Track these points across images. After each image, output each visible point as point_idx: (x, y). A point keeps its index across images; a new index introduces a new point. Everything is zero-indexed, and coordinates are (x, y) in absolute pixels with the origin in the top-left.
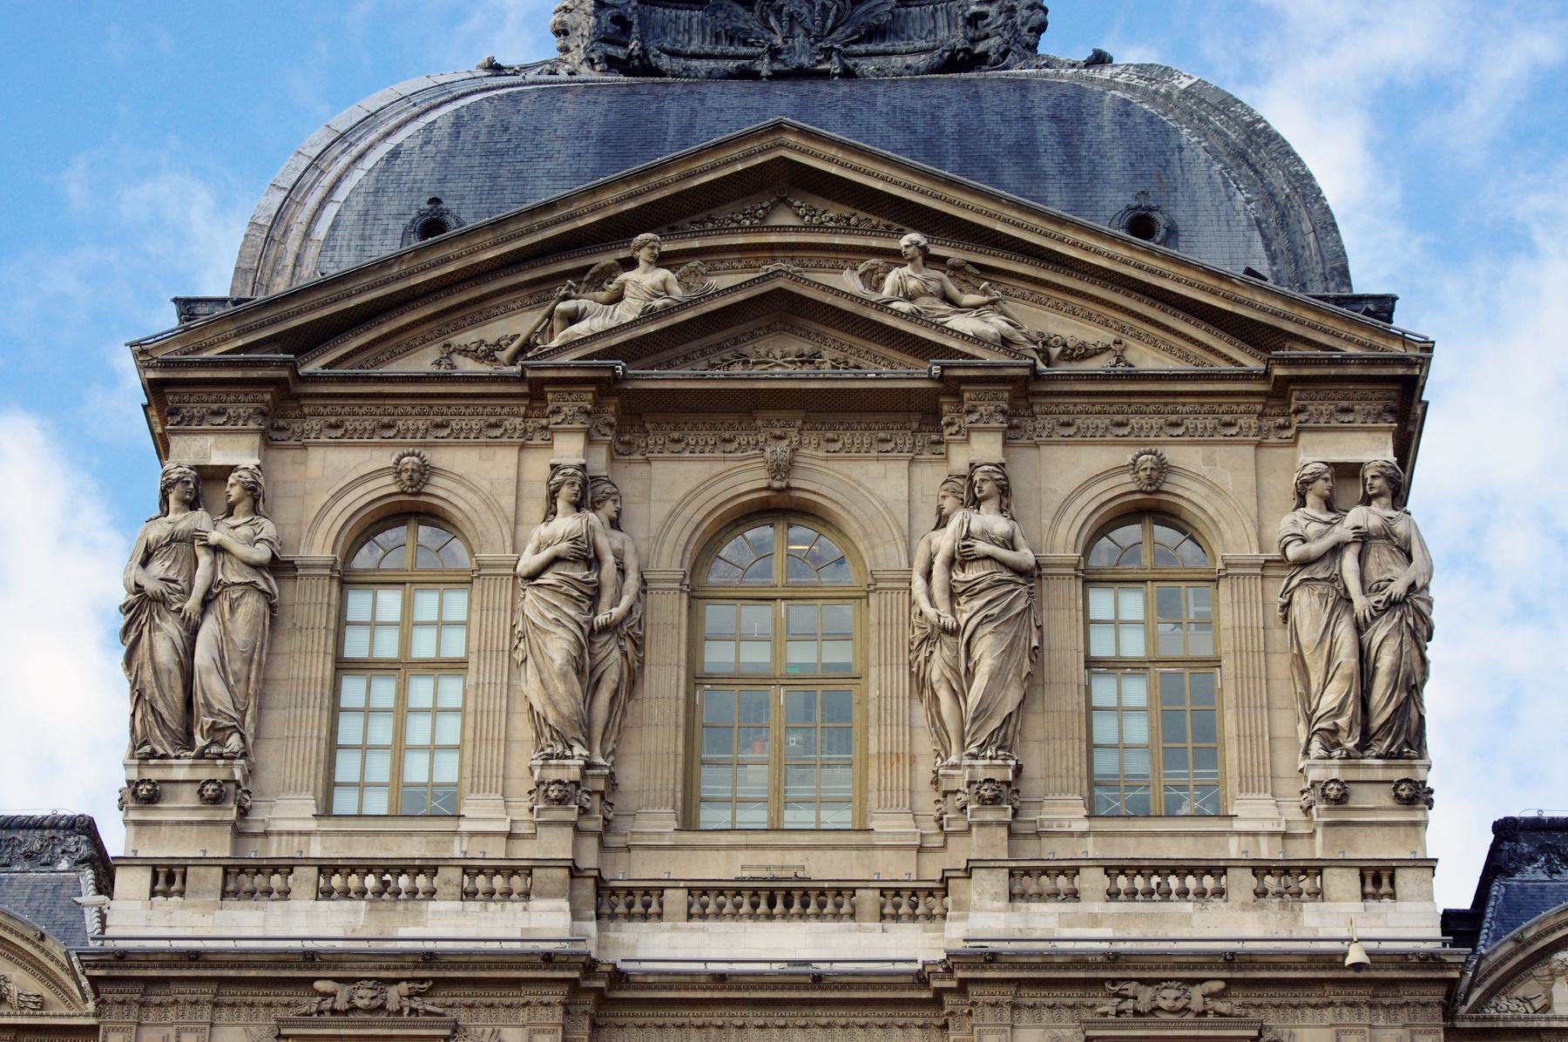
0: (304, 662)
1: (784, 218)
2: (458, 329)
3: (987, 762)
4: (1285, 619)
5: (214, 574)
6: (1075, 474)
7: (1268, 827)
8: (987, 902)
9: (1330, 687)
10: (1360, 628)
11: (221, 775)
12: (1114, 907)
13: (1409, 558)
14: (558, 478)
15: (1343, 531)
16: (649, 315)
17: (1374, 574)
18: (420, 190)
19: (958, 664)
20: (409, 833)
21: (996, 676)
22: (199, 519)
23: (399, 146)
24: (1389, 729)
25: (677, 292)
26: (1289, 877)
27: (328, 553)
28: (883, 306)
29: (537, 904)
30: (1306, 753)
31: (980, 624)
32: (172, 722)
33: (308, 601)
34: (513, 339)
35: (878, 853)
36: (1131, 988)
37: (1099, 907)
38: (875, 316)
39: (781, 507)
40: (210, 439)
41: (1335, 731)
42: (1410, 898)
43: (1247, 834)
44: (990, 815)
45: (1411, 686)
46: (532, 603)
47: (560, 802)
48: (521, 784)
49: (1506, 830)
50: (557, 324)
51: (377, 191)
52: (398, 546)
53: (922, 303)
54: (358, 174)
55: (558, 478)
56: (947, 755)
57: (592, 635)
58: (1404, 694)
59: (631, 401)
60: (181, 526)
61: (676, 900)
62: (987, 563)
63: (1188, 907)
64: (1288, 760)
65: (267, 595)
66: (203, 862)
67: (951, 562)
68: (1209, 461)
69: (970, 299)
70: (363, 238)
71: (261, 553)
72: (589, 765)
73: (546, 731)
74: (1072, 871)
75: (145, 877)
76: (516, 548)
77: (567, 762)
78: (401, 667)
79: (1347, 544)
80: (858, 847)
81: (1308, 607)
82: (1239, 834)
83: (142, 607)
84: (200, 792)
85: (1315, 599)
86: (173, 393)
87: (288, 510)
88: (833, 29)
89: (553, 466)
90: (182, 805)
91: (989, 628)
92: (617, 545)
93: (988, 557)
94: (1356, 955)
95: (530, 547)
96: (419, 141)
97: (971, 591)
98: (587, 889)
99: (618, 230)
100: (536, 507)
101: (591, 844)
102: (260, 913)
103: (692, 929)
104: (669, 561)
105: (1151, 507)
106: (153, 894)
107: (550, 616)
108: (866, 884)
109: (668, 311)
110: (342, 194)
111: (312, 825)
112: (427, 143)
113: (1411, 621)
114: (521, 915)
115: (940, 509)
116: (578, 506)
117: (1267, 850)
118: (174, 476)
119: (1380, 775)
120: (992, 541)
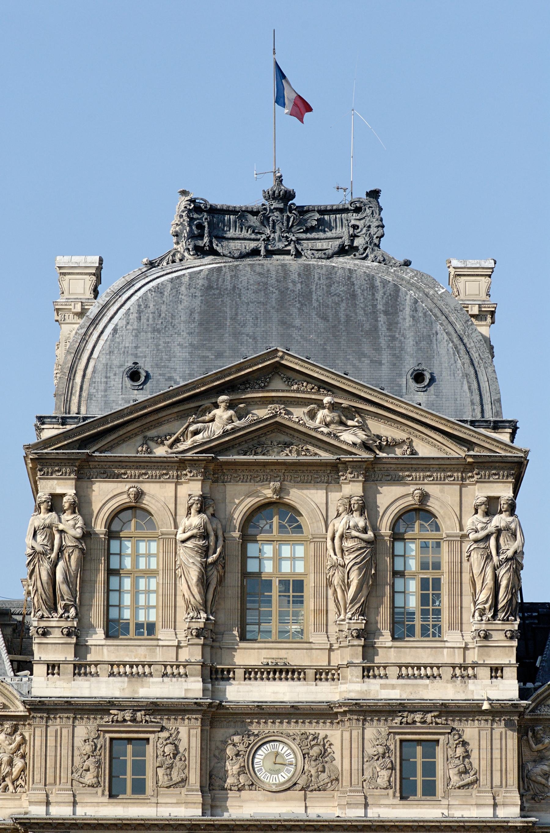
2: (149, 429)
3: (355, 621)
4: (468, 560)
5: (62, 542)
7: (458, 645)
8: (355, 679)
9: (483, 592)
10: (495, 569)
11: (69, 624)
12: (401, 681)
13: (515, 539)
14: (191, 501)
15: (491, 528)
16: (226, 433)
17: (503, 547)
18: (128, 352)
19: (344, 580)
20: (140, 646)
21: (359, 589)
23: (117, 325)
25: (238, 423)
26: (463, 671)
27: (103, 529)
28: (316, 429)
29: (190, 679)
30: (473, 616)
31: (353, 565)
34: (171, 435)
35: (313, 651)
36: (405, 714)
37: (395, 681)
38: (314, 434)
40: (56, 481)
41: (484, 609)
42: (508, 679)
43: (450, 648)
44: (356, 642)
47: (198, 636)
48: (182, 626)
50: (189, 435)
51: (110, 352)
53: (333, 426)
54: (101, 342)
55: (191, 501)
56: (340, 615)
57: (205, 567)
58: (510, 596)
60: (47, 522)
61: (240, 673)
62: (356, 539)
63: (427, 681)
64: (466, 616)
65: (82, 550)
66: (66, 662)
67: (342, 537)
68: (442, 491)
69: (350, 423)
70: (106, 377)
71: (78, 532)
72: (208, 619)
73: (190, 606)
74: (385, 667)
75: (45, 667)
76: (176, 527)
77: (199, 620)
79: (492, 534)
80: (307, 649)
82: (447, 648)
84: (62, 631)
85: (479, 556)
88: (292, 226)
89: (190, 495)
91: (356, 567)
92: (214, 526)
93: (356, 537)
94: (486, 706)
95: (180, 530)
96: (124, 322)
97: (351, 551)
98: (208, 672)
100: (182, 510)
101: (208, 649)
102: (88, 682)
103: (246, 684)
106: (48, 674)
107: (191, 561)
108: (310, 667)
109: (234, 430)
110: (95, 355)
111: (103, 642)
112: (128, 323)
113: (514, 566)
114: (184, 683)
115: (338, 510)
116: (199, 512)
118: (44, 500)
119: (500, 627)
120: (358, 531)
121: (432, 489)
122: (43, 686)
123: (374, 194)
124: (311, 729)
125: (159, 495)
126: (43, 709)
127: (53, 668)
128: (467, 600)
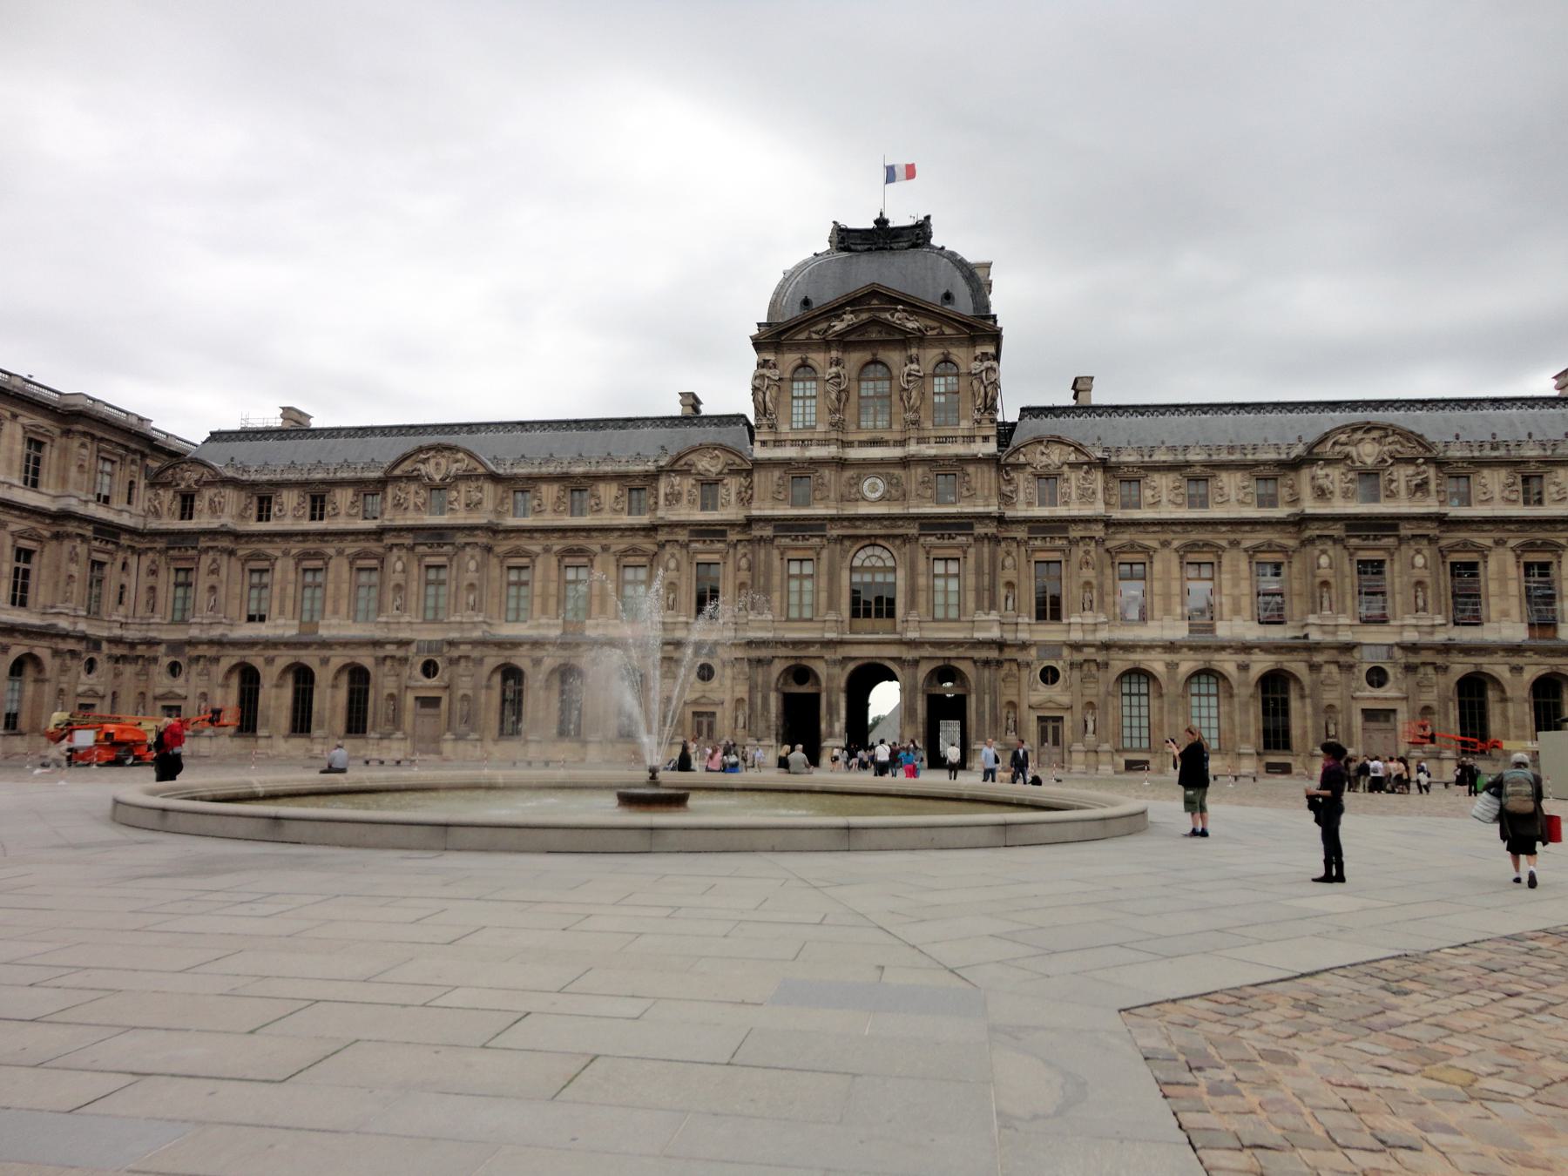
0: (786, 398)
1: (875, 302)
6: (932, 355)
22: (764, 371)
24: (990, 407)
26: (970, 439)
32: (762, 410)
33: (785, 385)
39: (875, 362)
45: (994, 399)
46: (828, 387)
49: (1023, 410)
52: (801, 373)
59: (844, 342)
78: (804, 398)
81: (975, 383)
83: (755, 389)
86: (758, 344)
87: (780, 367)
90: (764, 429)
99: (842, 306)
104: (854, 375)
105: (946, 360)
117: (966, 433)
121: (953, 351)
122: (760, 453)
123: (928, 218)
124: (892, 471)
125: (817, 358)
126: (759, 464)
127: (764, 443)
128: (970, 405)
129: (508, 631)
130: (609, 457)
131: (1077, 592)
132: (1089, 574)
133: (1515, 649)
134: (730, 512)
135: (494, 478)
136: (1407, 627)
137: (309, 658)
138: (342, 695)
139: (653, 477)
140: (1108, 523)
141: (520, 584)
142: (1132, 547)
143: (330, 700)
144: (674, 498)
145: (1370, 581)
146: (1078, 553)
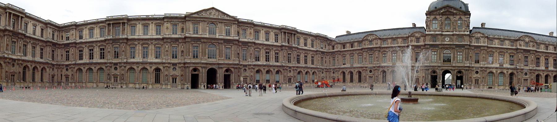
129: (383, 65)
130: (400, 34)
131: (482, 58)
132: (484, 55)
133: (543, 71)
134: (421, 43)
135: (380, 39)
136: (531, 66)
137: (352, 70)
138: (357, 76)
139: (408, 37)
140: (488, 47)
141: (385, 57)
142: (491, 51)
143: (356, 77)
144: (411, 41)
145: (526, 60)
146: (482, 52)
